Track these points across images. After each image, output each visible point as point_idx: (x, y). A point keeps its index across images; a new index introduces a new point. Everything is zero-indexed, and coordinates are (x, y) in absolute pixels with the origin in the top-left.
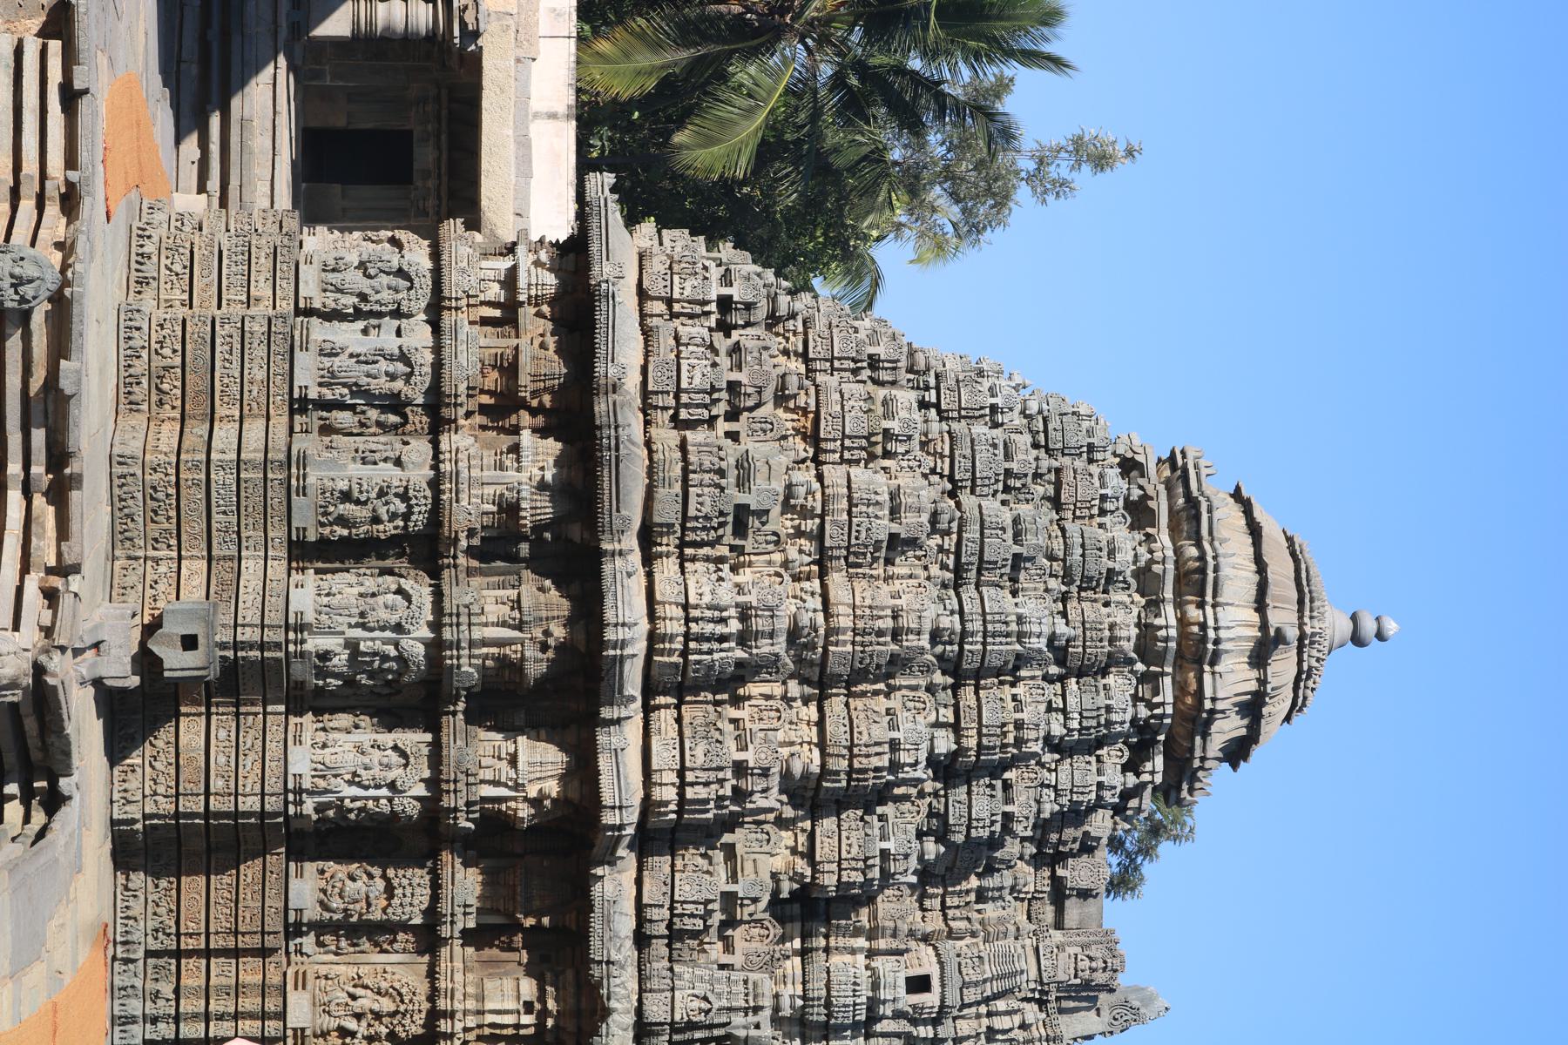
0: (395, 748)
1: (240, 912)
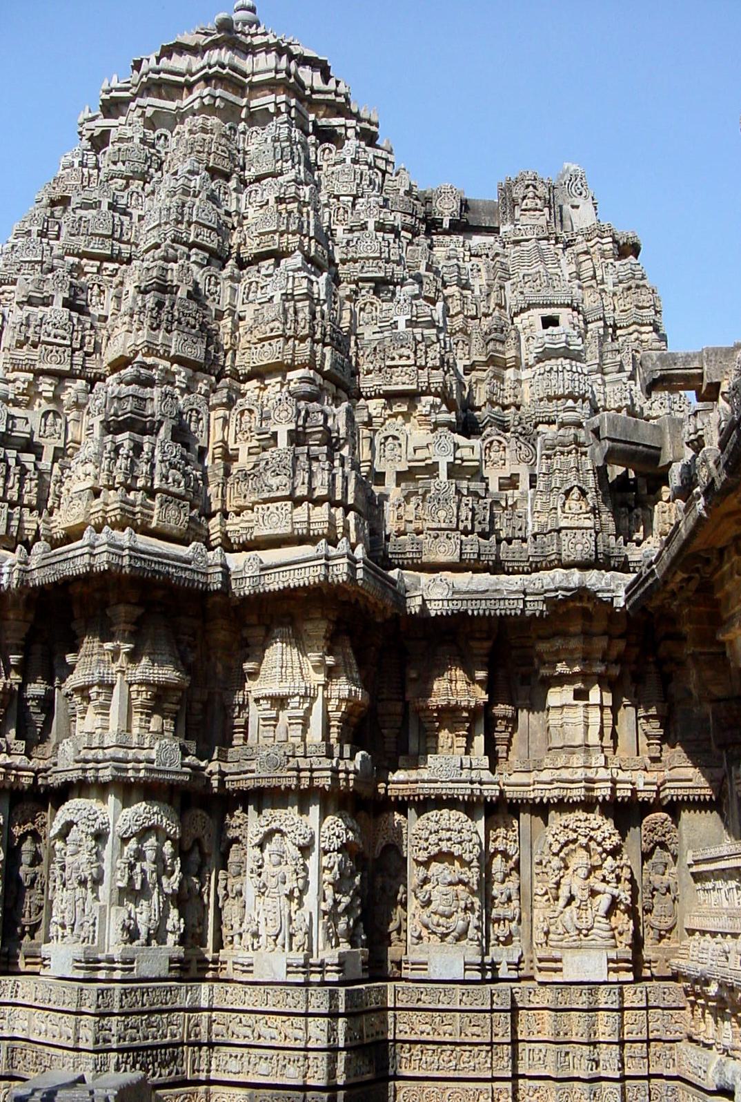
0: (261, 846)
1: (467, 1040)
